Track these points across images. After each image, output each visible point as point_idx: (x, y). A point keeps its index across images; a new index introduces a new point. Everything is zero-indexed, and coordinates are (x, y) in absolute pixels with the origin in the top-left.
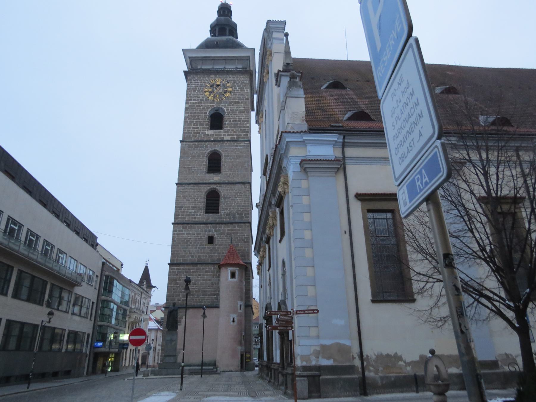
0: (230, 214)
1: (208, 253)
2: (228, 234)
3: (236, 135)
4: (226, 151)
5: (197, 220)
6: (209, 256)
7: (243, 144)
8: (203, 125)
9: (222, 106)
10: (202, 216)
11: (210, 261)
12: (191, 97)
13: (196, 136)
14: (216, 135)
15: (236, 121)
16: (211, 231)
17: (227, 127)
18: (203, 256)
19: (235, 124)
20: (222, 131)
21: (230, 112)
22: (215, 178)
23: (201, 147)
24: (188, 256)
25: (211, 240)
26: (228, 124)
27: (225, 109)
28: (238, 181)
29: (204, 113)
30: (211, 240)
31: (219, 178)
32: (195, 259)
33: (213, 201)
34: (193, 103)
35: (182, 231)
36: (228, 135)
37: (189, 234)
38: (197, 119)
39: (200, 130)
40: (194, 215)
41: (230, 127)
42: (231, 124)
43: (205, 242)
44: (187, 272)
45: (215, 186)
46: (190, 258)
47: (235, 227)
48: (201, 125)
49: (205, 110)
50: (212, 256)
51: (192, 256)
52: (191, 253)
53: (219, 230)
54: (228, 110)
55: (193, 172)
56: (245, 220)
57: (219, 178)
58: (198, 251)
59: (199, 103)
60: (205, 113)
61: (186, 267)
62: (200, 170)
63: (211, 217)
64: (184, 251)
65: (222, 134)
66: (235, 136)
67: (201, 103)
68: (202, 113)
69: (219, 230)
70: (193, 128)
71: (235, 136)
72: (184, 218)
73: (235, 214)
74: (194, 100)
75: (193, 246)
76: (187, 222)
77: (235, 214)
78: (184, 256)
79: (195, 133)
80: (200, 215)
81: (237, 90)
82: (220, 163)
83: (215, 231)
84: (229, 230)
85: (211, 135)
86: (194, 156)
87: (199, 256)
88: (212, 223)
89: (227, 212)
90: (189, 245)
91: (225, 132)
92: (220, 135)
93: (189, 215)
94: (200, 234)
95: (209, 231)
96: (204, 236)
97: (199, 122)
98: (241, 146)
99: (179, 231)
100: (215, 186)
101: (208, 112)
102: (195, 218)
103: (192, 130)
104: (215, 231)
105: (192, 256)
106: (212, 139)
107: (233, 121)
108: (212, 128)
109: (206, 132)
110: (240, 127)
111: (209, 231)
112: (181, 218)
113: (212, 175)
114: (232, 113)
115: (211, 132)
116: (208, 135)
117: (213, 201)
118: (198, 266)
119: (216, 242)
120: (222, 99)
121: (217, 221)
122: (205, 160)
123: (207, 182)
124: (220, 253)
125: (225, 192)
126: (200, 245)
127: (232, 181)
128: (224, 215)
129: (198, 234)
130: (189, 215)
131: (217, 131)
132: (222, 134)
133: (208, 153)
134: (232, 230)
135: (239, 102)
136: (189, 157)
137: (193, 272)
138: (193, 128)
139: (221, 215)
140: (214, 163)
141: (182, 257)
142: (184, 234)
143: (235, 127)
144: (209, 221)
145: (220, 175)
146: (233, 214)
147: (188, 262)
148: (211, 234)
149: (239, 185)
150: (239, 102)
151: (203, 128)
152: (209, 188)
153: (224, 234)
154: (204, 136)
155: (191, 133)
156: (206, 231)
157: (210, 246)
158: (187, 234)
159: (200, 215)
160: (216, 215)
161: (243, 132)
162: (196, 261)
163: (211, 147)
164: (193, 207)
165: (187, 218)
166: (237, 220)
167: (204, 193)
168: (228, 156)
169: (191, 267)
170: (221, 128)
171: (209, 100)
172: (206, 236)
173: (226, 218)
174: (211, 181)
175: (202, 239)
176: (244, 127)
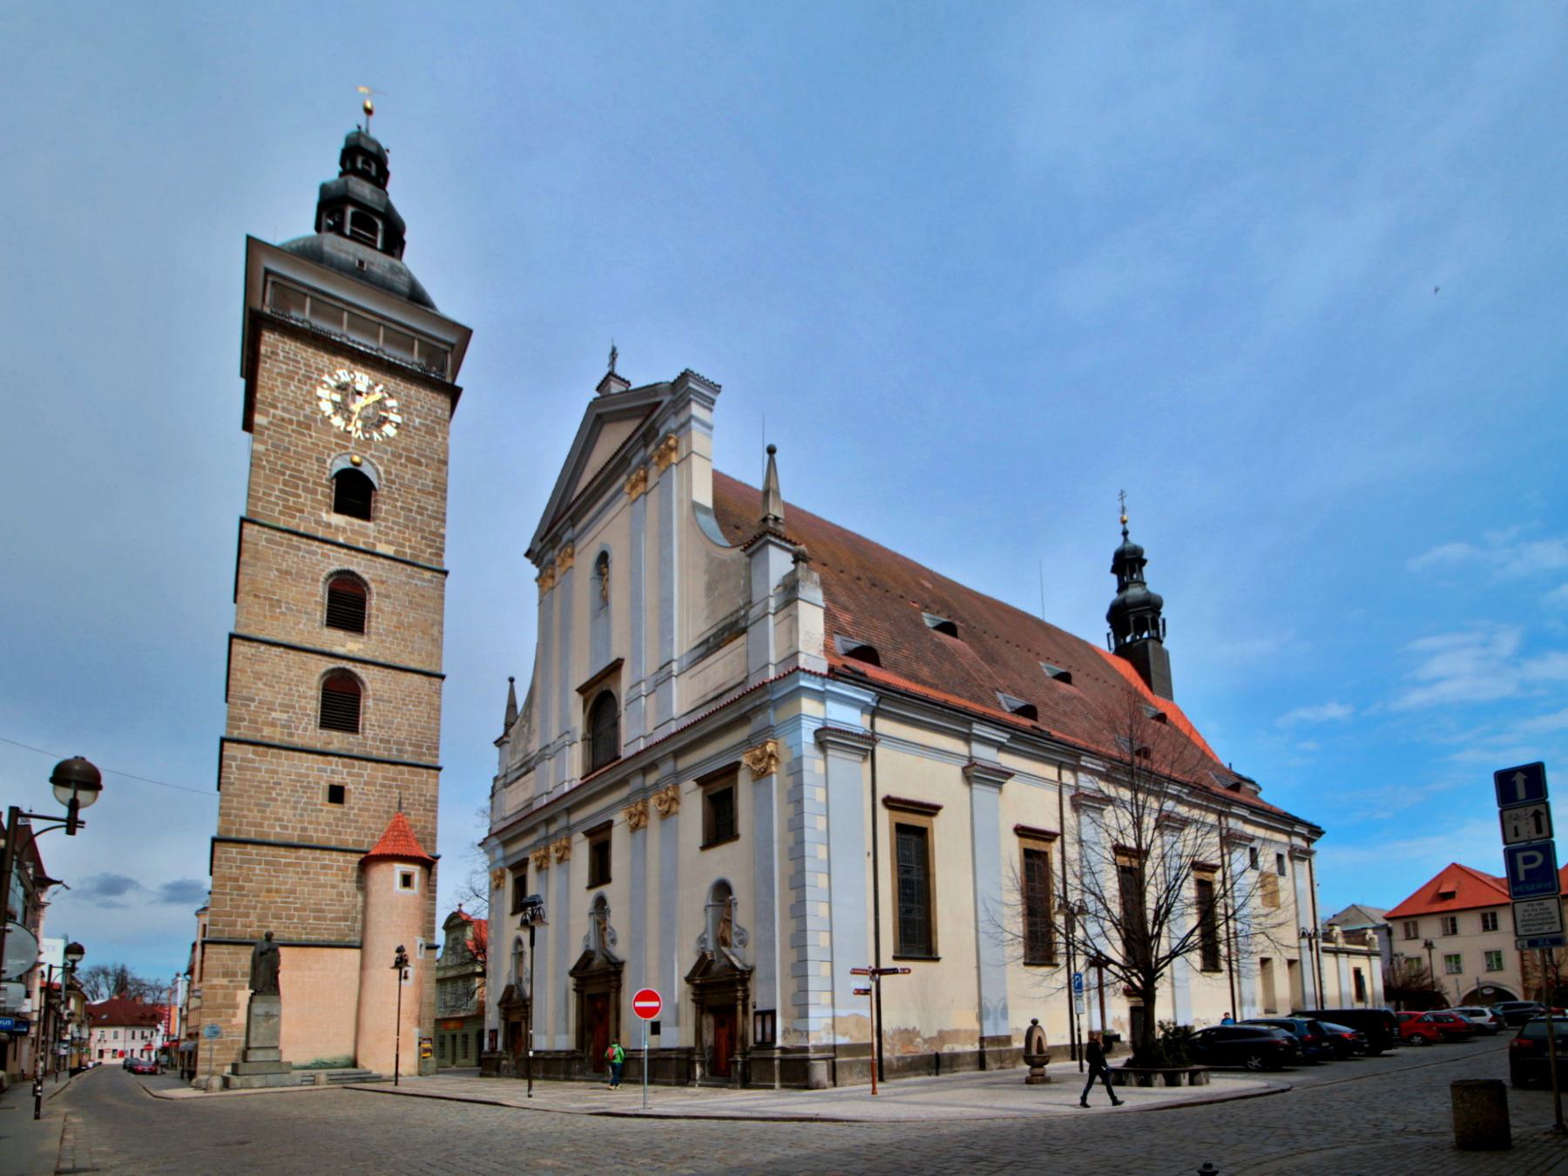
0: (388, 742)
1: (328, 824)
2: (383, 785)
4: (382, 582)
5: (297, 741)
6: (332, 832)
7: (427, 575)
8: (315, 492)
10: (310, 731)
11: (333, 844)
12: (275, 399)
16: (338, 772)
17: (385, 520)
18: (316, 830)
19: (407, 518)
20: (371, 525)
21: (393, 482)
22: (347, 644)
23: (308, 552)
24: (273, 826)
25: (337, 794)
28: (413, 665)
29: (318, 460)
30: (337, 794)
31: (361, 646)
32: (294, 836)
33: (341, 702)
34: (283, 420)
36: (390, 543)
37: (276, 772)
42: (398, 515)
43: (322, 796)
44: (267, 863)
45: (349, 666)
47: (402, 773)
48: (306, 489)
50: (340, 833)
51: (285, 827)
53: (361, 775)
56: (426, 760)
57: (361, 646)
59: (299, 424)
60: (321, 461)
61: (265, 850)
63: (337, 740)
66: (408, 551)
67: (308, 427)
68: (310, 457)
69: (361, 775)
71: (408, 551)
73: (403, 744)
74: (284, 409)
75: (286, 801)
77: (403, 744)
78: (261, 825)
80: (305, 729)
82: (363, 607)
83: (349, 774)
84: (385, 778)
85: (337, 528)
87: (304, 829)
88: (340, 756)
89: (383, 734)
92: (367, 536)
94: (308, 776)
98: (423, 580)
100: (349, 666)
104: (349, 774)
106: (341, 540)
108: (339, 509)
110: (422, 530)
111: (333, 772)
113: (340, 634)
116: (329, 525)
117: (341, 702)
118: (302, 852)
119: (351, 799)
120: (371, 438)
121: (355, 752)
122: (321, 592)
123: (326, 649)
124: (362, 828)
125: (378, 685)
127: (397, 662)
128: (374, 739)
133: (331, 575)
134: (394, 780)
137: (287, 865)
139: (365, 738)
140: (347, 604)
141: (254, 825)
144: (332, 748)
146: (396, 743)
147: (272, 839)
148: (337, 780)
149: (416, 677)
151: (313, 500)
152: (331, 666)
153: (374, 784)
156: (325, 771)
157: (335, 807)
159: (305, 729)
160: (350, 738)
162: (295, 841)
163: (337, 559)
166: (406, 758)
168: (388, 596)
169: (282, 851)
171: (332, 426)
172: (324, 784)
174: (338, 650)
176: (431, 533)
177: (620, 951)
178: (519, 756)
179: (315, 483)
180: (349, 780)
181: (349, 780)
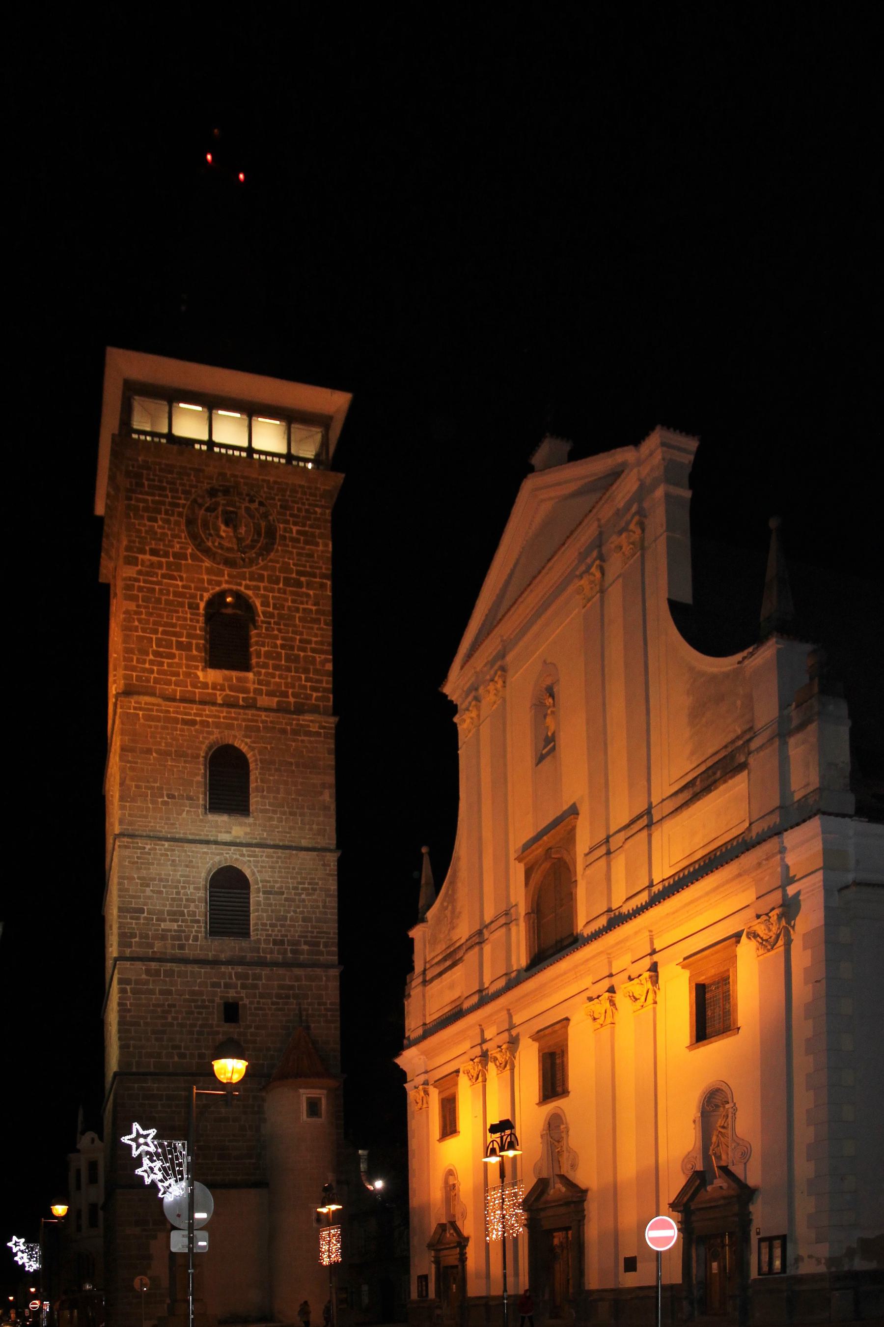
3: (295, 695)
9: (247, 587)
13: (169, 683)
14: (231, 688)
15: (292, 648)
17: (265, 666)
19: (288, 659)
20: (250, 675)
21: (272, 616)
26: (268, 655)
27: (258, 603)
31: (248, 830)
35: (147, 983)
36: (270, 694)
37: (169, 993)
38: (166, 625)
39: (179, 665)
40: (179, 938)
41: (276, 667)
46: (176, 1059)
49: (193, 596)
51: (182, 1056)
52: (179, 1047)
54: (265, 604)
55: (165, 803)
58: (198, 1040)
60: (194, 607)
62: (190, 798)
63: (229, 947)
64: (157, 1039)
65: (252, 687)
66: (292, 700)
70: (157, 654)
71: (292, 700)
72: (151, 946)
76: (158, 956)
79: (164, 673)
81: (293, 540)
83: (243, 987)
86: (167, 753)
90: (171, 1025)
91: (260, 683)
92: (245, 690)
93: (163, 938)
94: (201, 993)
95: (227, 986)
96: (213, 1001)
97: (175, 634)
99: (137, 982)
101: (202, 605)
102: (182, 947)
103: (152, 662)
104: (243, 987)
105: (182, 1056)
107: (283, 647)
108: (213, 662)
109: (200, 674)
110: (306, 671)
111: (227, 986)
112: (140, 945)
114: (281, 617)
115: (213, 676)
116: (205, 685)
126: (201, 1026)
129: (193, 993)
130: (163, 938)
131: (234, 674)
132: (252, 687)
135: (299, 584)
136: (149, 751)
138: (157, 654)
142: (152, 992)
143: (289, 669)
145: (251, 820)
150: (299, 584)
151: (190, 658)
154: (194, 686)
155: (152, 671)
158: (162, 992)
160: (244, 944)
161: (314, 689)
164: (174, 913)
165: (158, 946)
167: (203, 875)
170: (246, 667)
173: (272, 952)
174: (224, 837)
175: (206, 1007)
177: (587, 1176)
178: (440, 947)
179: (189, 636)
180: (243, 993)
181: (243, 993)
